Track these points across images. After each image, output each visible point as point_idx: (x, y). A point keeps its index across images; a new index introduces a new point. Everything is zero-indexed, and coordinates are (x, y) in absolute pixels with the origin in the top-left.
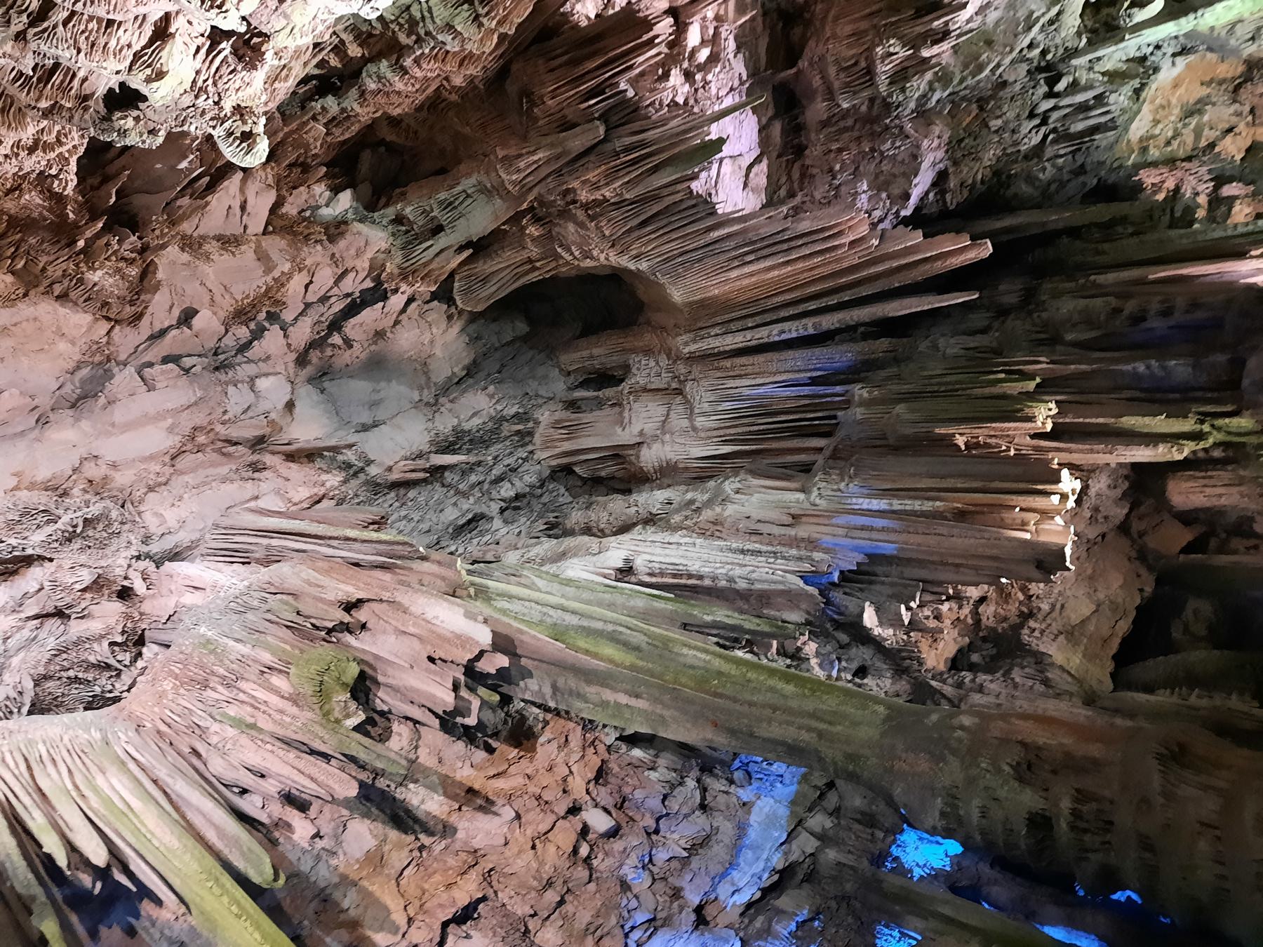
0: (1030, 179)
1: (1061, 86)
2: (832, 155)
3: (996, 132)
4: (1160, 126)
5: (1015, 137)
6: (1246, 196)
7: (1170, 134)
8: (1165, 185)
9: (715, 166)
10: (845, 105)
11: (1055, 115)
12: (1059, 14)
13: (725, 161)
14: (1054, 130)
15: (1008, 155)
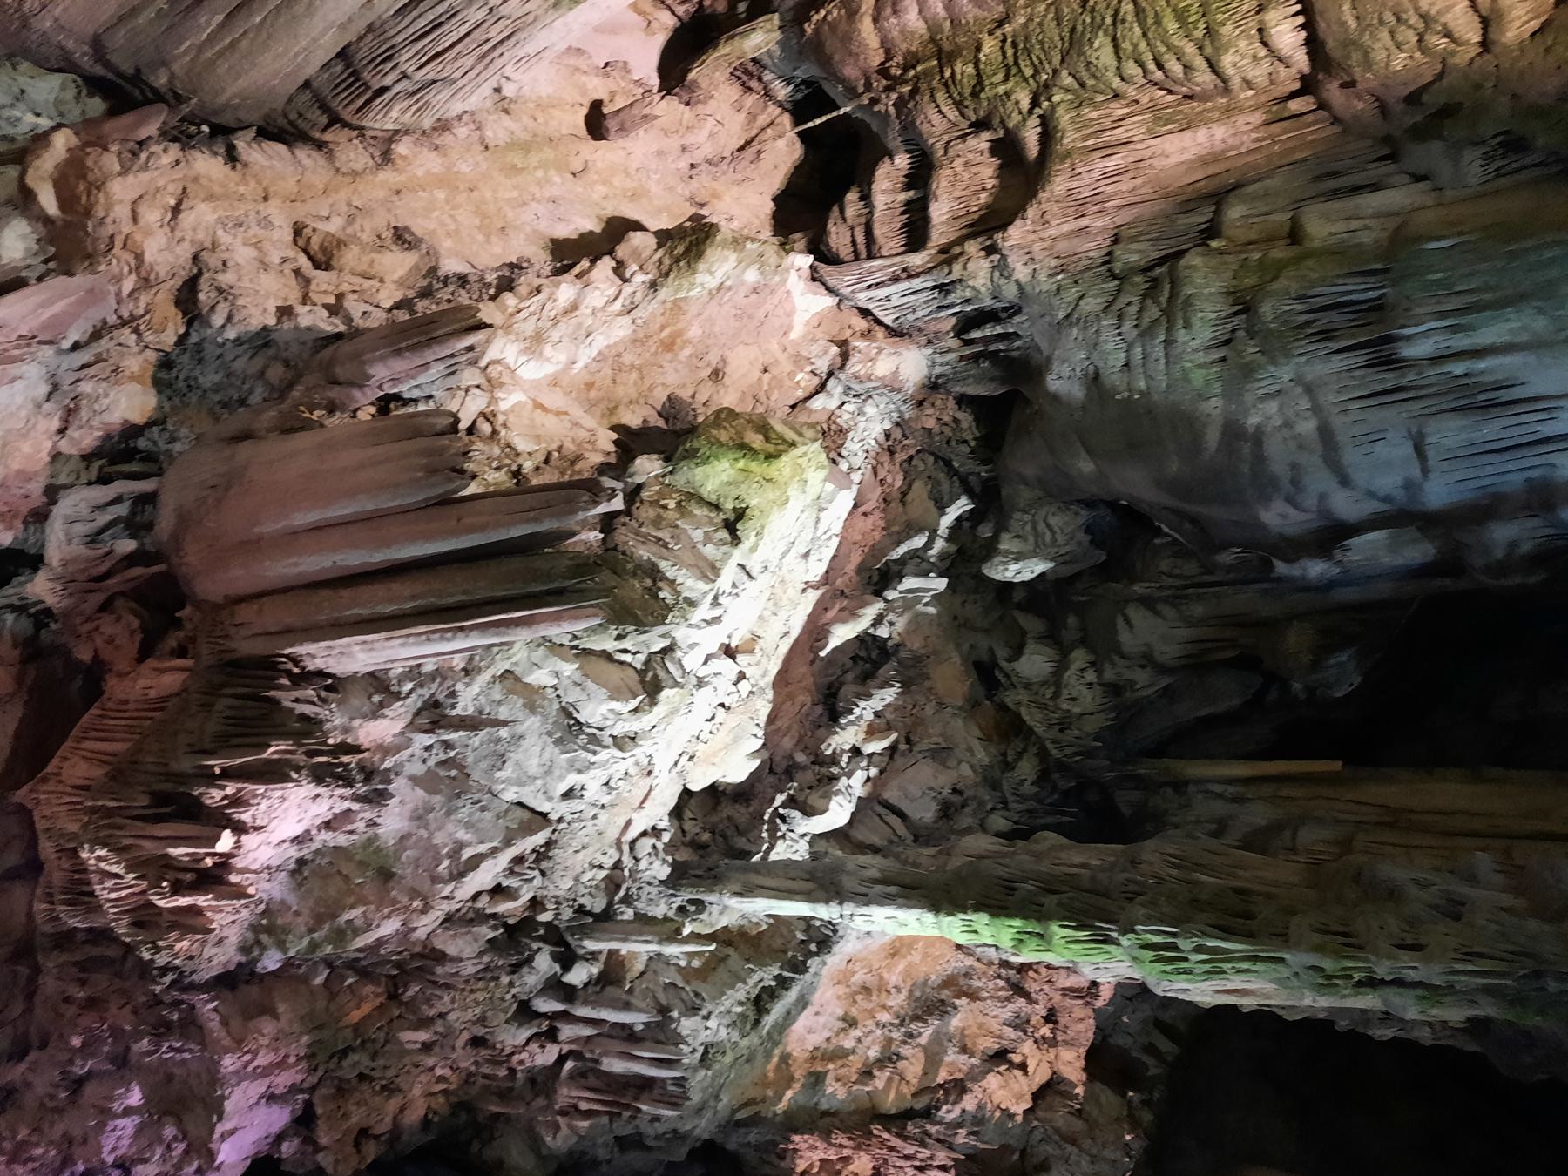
4: (857, 1033)
7: (873, 1053)
11: (567, 1031)
12: (549, 844)
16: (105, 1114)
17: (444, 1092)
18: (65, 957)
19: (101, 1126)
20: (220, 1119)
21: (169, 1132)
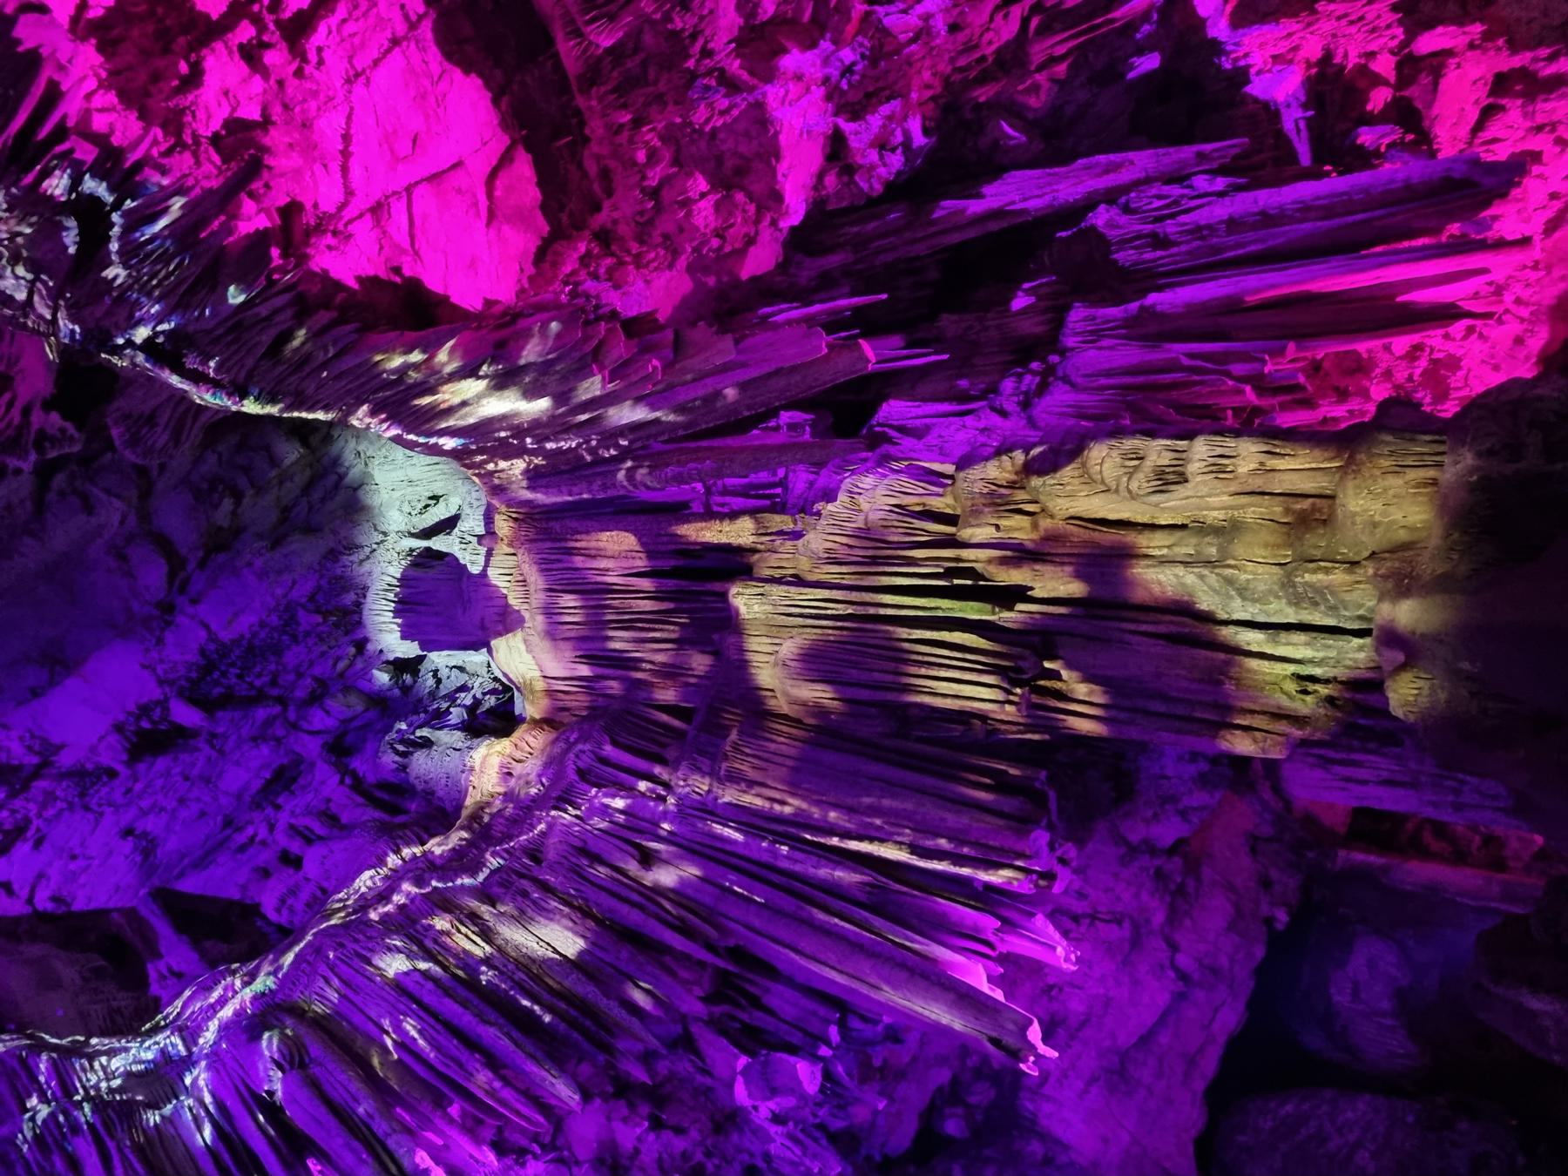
0: (1015, 112)
2: (626, 134)
3: (913, 40)
6: (1471, 46)
8: (1302, 54)
10: (609, 43)
13: (418, 192)
15: (962, 70)
16: (687, 203)
17: (933, 98)
18: (603, 89)
19: (689, 214)
20: (778, 160)
21: (740, 197)
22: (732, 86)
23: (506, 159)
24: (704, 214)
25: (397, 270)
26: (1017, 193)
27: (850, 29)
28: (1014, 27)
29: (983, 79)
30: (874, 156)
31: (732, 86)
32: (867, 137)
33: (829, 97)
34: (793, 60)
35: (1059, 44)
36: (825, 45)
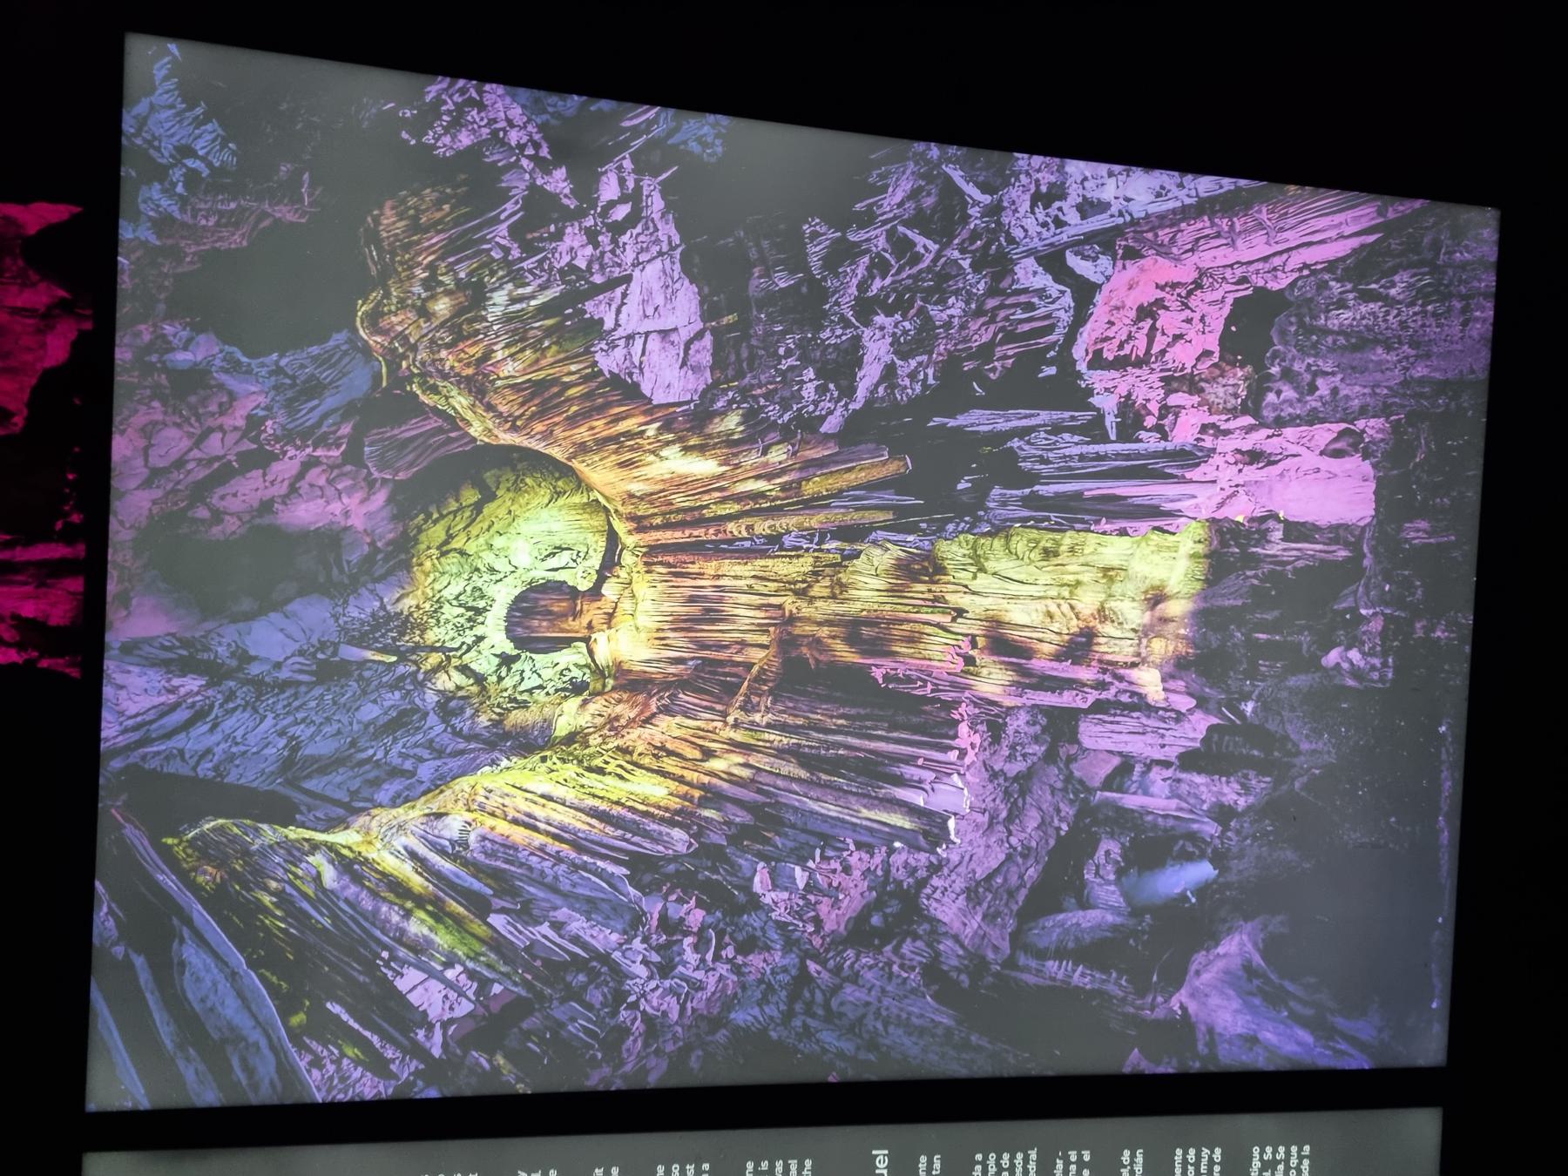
1: (1004, 284)
4: (1114, 329)
5: (964, 333)
9: (639, 342)
10: (783, 285)
13: (651, 337)
14: (1002, 329)
22: (847, 324)
23: (699, 335)
24: (809, 392)
25: (631, 375)
26: (978, 420)
27: (913, 312)
28: (990, 335)
29: (969, 358)
30: (907, 382)
31: (847, 324)
32: (907, 371)
33: (892, 344)
34: (880, 319)
35: (1011, 349)
36: (898, 317)
